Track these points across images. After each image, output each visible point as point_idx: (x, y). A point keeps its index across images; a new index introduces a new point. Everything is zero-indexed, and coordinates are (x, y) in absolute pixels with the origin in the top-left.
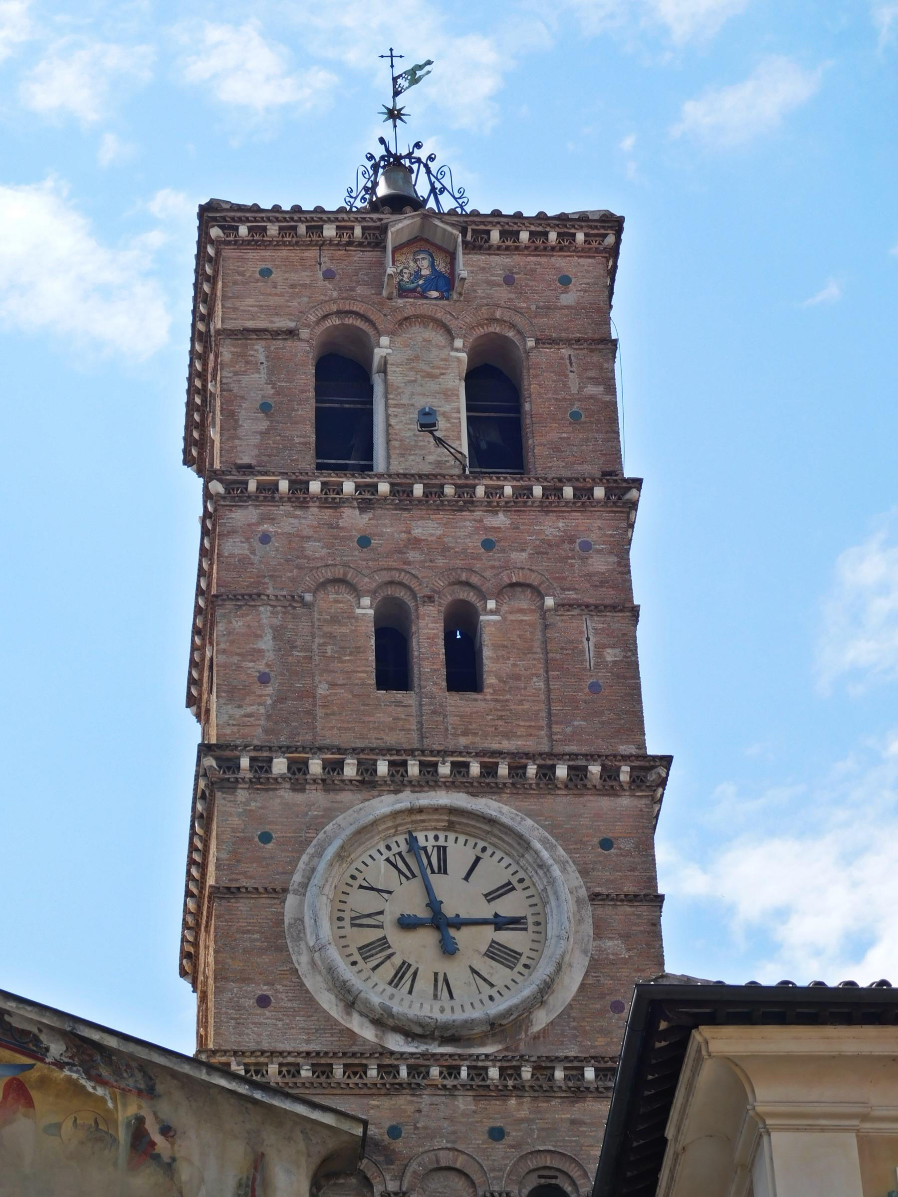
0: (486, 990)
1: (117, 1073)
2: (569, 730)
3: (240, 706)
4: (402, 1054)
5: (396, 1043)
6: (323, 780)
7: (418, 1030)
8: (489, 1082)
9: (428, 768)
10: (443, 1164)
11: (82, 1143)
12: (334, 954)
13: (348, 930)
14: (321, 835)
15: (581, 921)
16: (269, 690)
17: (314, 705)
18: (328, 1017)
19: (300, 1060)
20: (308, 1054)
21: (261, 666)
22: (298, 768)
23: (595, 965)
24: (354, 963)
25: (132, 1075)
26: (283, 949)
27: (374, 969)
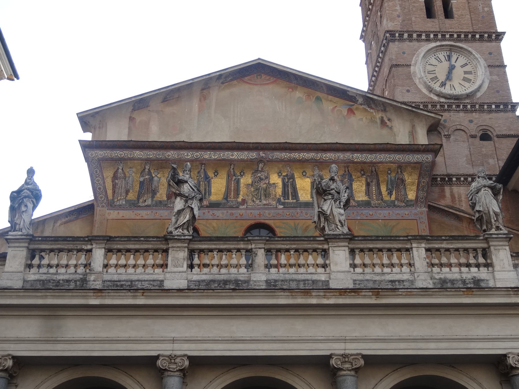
0: (464, 88)
1: (376, 106)
2: (477, 27)
3: (393, 23)
4: (446, 102)
5: (442, 100)
6: (417, 39)
7: (449, 97)
8: (468, 109)
9: (443, 36)
10: (458, 128)
11: (368, 123)
12: (425, 78)
13: (427, 74)
14: (418, 52)
15: (486, 72)
16: (400, 19)
17: (412, 22)
18: (425, 94)
19: (420, 104)
20: (422, 102)
21: (397, 13)
22: (410, 36)
23: (491, 82)
24: (430, 82)
25: (380, 106)
26: (411, 79)
27: (435, 84)
